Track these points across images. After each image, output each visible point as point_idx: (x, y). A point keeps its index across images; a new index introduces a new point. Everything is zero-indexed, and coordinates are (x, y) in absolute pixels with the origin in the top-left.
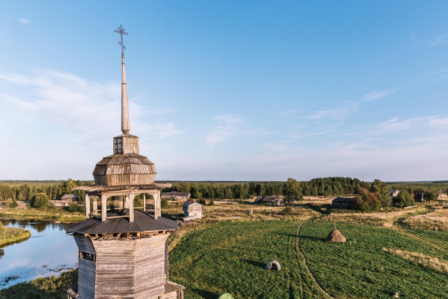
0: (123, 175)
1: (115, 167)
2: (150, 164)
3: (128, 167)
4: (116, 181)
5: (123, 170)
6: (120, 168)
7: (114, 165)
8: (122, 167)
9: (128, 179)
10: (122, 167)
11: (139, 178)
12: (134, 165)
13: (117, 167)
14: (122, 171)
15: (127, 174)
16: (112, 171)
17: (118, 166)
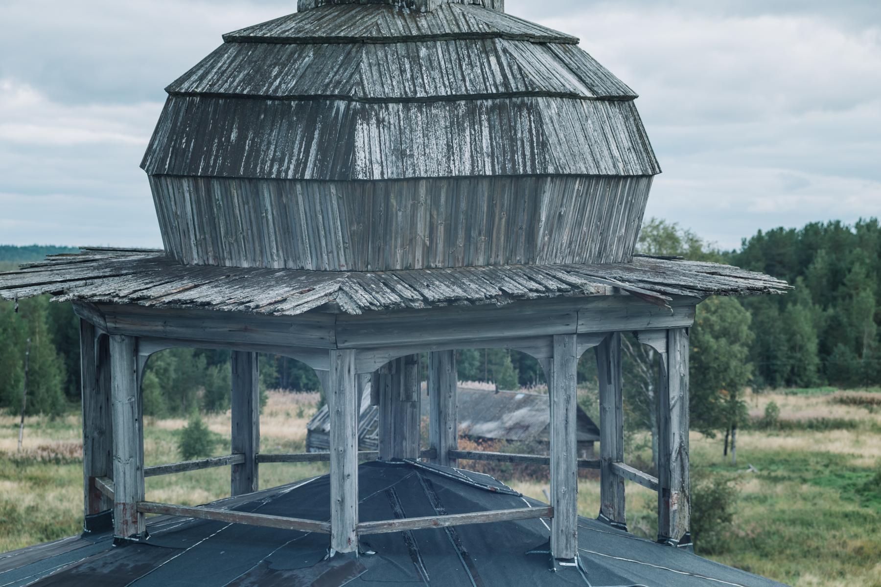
0: (484, 188)
1: (419, 118)
2: (623, 100)
3: (524, 124)
4: (421, 229)
5: (486, 143)
6: (455, 126)
7: (406, 101)
8: (472, 113)
9: (523, 219)
10: (472, 113)
11: (582, 210)
12: (554, 103)
13: (431, 122)
14: (476, 150)
15: (516, 178)
16: (401, 154)
17: (439, 112)
